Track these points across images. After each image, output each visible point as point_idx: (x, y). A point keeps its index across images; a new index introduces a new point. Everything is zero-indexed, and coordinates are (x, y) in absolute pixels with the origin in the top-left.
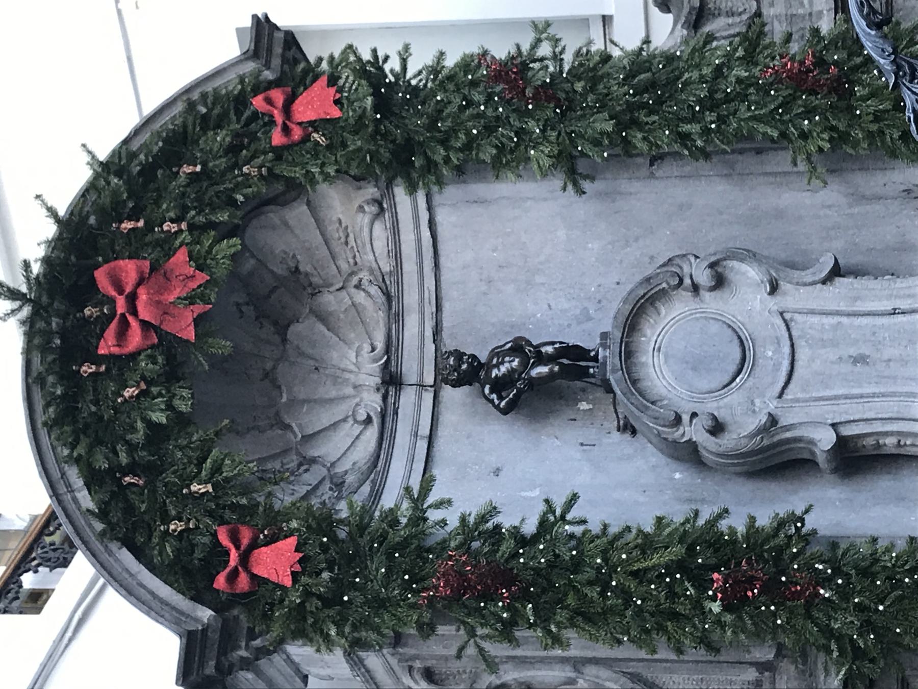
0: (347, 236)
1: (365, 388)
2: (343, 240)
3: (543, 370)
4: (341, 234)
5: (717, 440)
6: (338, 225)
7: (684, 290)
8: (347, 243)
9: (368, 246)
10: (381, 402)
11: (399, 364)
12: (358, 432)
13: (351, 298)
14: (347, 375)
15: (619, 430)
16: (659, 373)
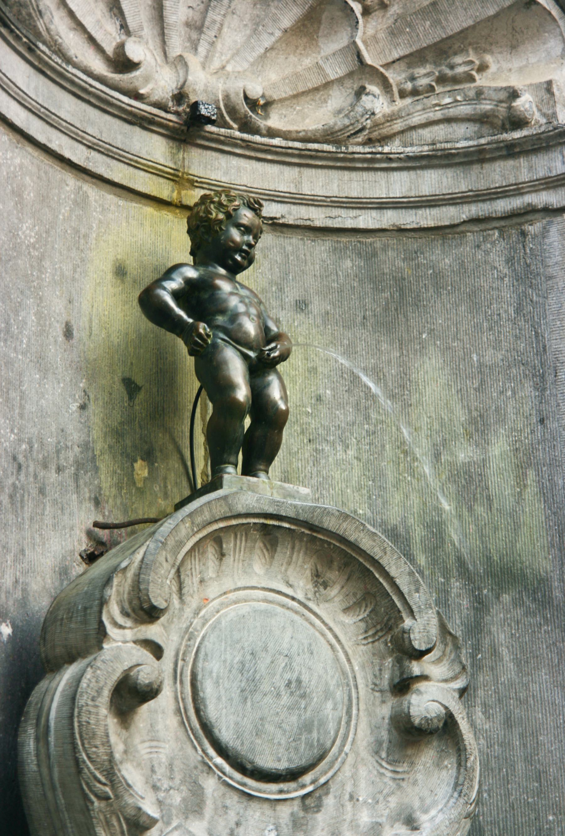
0: (455, 80)
1: (181, 73)
2: (449, 72)
3: (236, 369)
4: (461, 70)
5: (106, 693)
6: (477, 62)
7: (399, 661)
8: (442, 80)
9: (439, 115)
10: (155, 98)
11: (223, 146)
12: (104, 45)
13: (340, 81)
14: (202, 49)
15: (96, 524)
16: (232, 596)
